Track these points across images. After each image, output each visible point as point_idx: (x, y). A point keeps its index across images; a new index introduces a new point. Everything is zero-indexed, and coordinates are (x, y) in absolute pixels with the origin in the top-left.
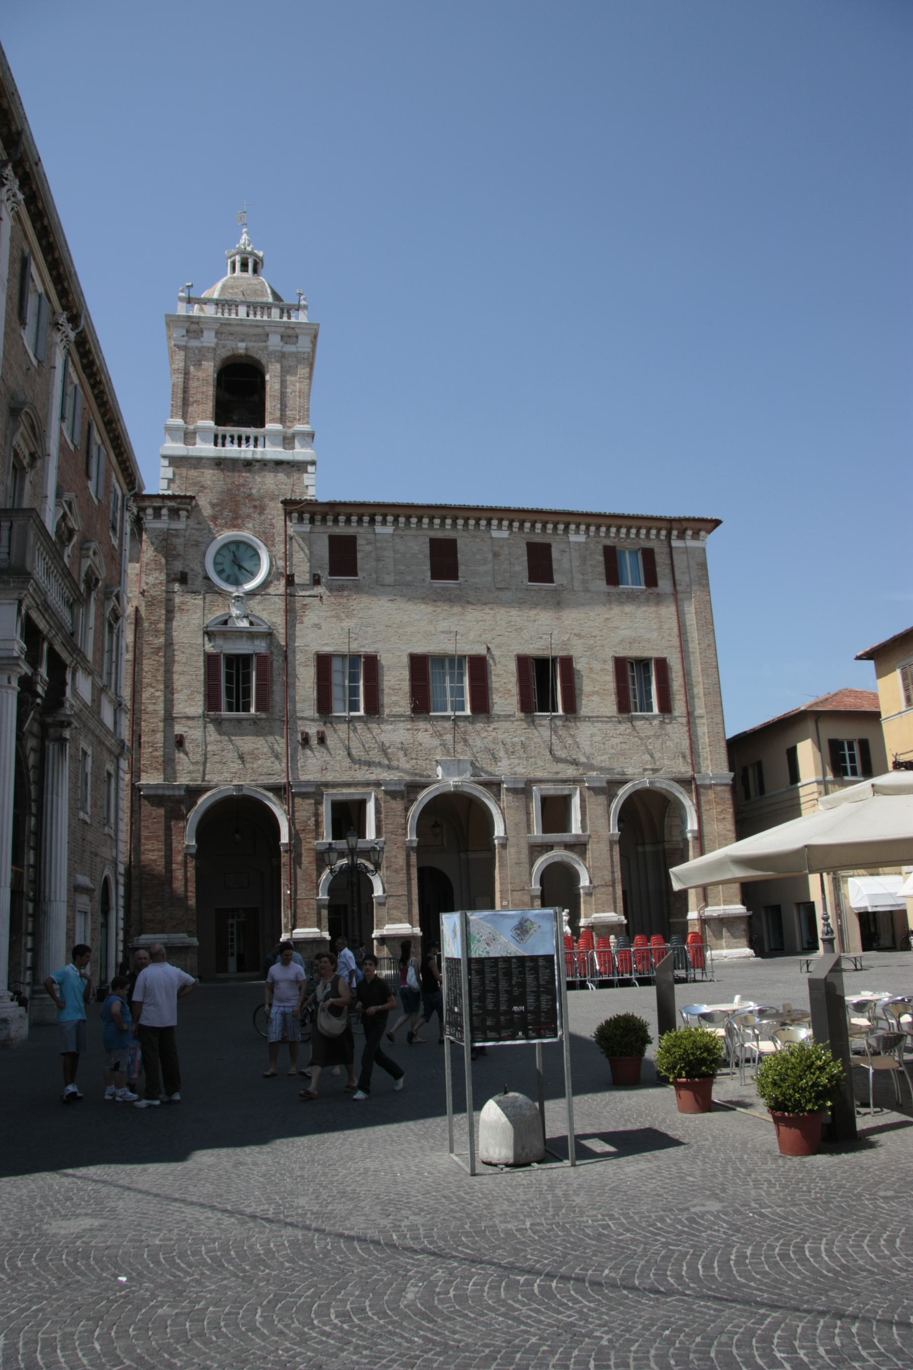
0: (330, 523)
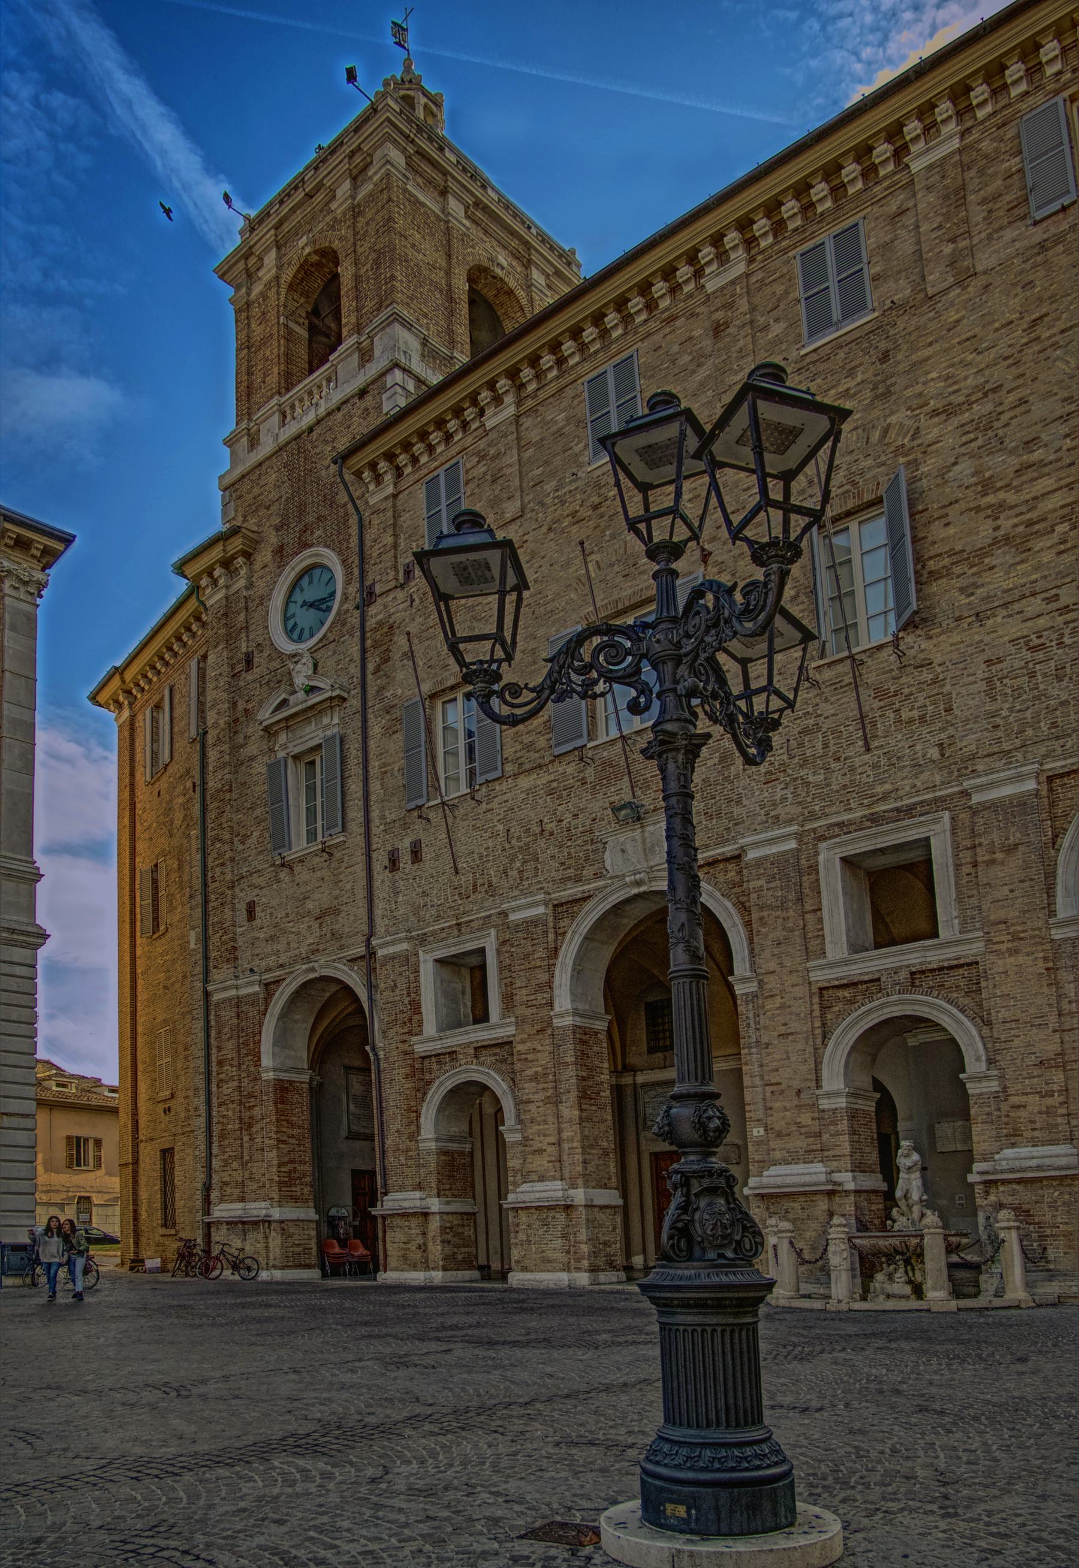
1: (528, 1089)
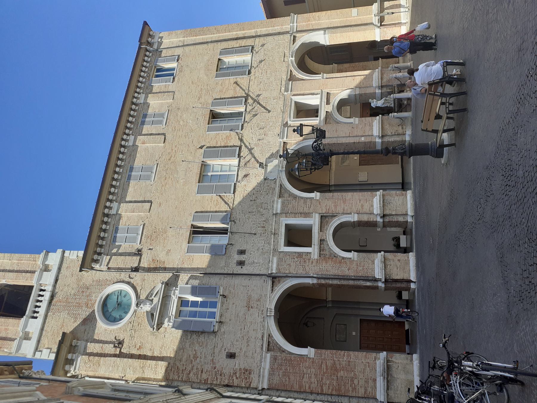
0: (104, 243)
1: (339, 209)
